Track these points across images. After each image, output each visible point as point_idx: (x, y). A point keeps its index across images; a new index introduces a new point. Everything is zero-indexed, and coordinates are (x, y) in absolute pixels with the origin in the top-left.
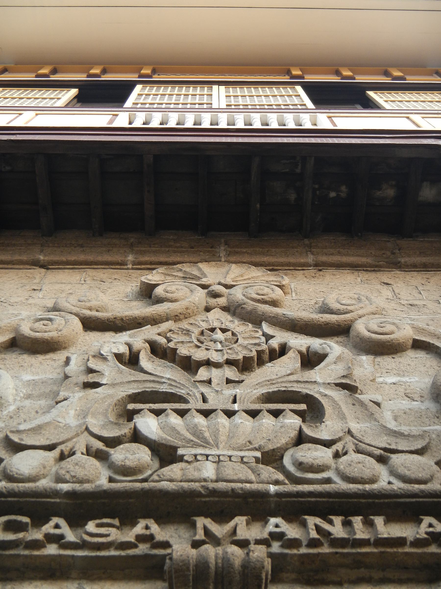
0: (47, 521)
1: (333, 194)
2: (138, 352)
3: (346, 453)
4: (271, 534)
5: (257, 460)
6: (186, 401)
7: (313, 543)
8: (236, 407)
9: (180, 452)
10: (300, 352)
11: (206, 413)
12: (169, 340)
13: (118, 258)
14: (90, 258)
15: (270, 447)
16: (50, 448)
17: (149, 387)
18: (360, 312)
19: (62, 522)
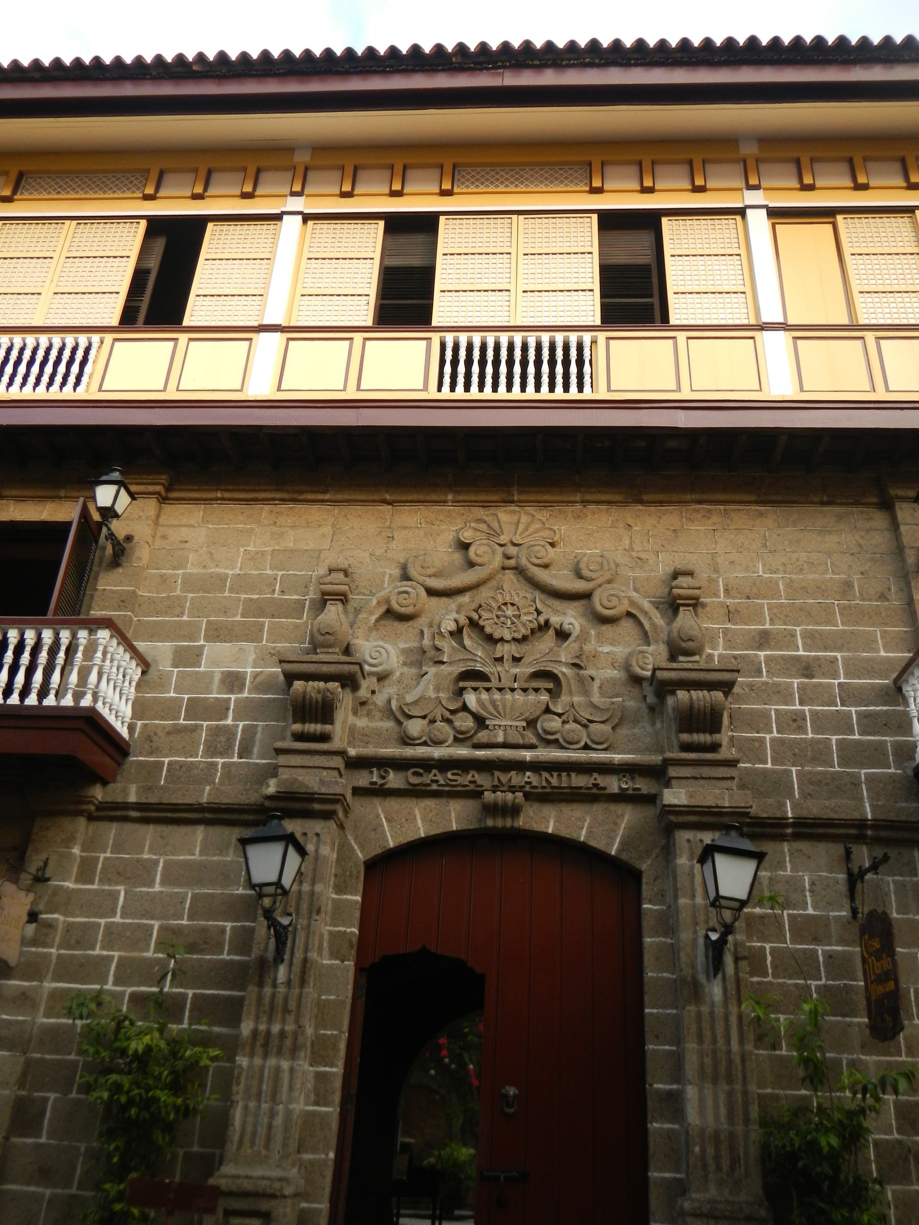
0: (430, 772)
1: (599, 445)
2: (463, 628)
3: (568, 722)
4: (527, 783)
5: (524, 728)
6: (489, 680)
7: (543, 787)
8: (516, 685)
9: (487, 722)
10: (556, 630)
11: (500, 690)
12: (480, 617)
13: (441, 498)
14: (421, 497)
15: (531, 718)
16: (424, 717)
17: (470, 666)
18: (599, 581)
19: (437, 773)
